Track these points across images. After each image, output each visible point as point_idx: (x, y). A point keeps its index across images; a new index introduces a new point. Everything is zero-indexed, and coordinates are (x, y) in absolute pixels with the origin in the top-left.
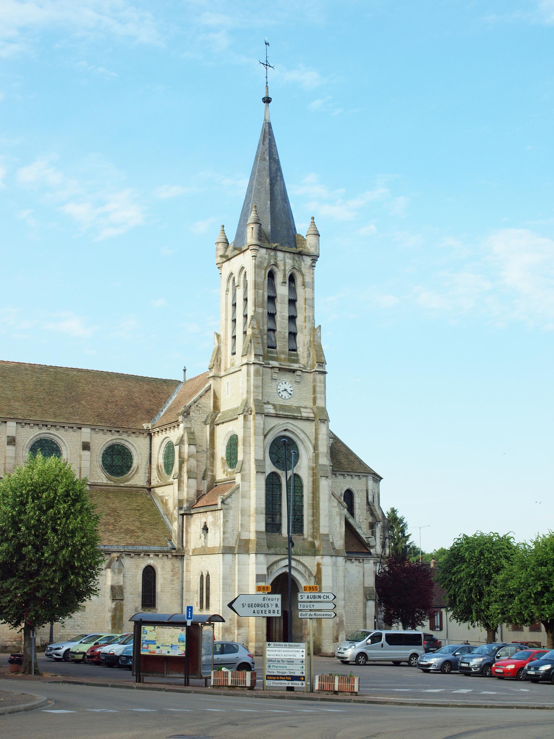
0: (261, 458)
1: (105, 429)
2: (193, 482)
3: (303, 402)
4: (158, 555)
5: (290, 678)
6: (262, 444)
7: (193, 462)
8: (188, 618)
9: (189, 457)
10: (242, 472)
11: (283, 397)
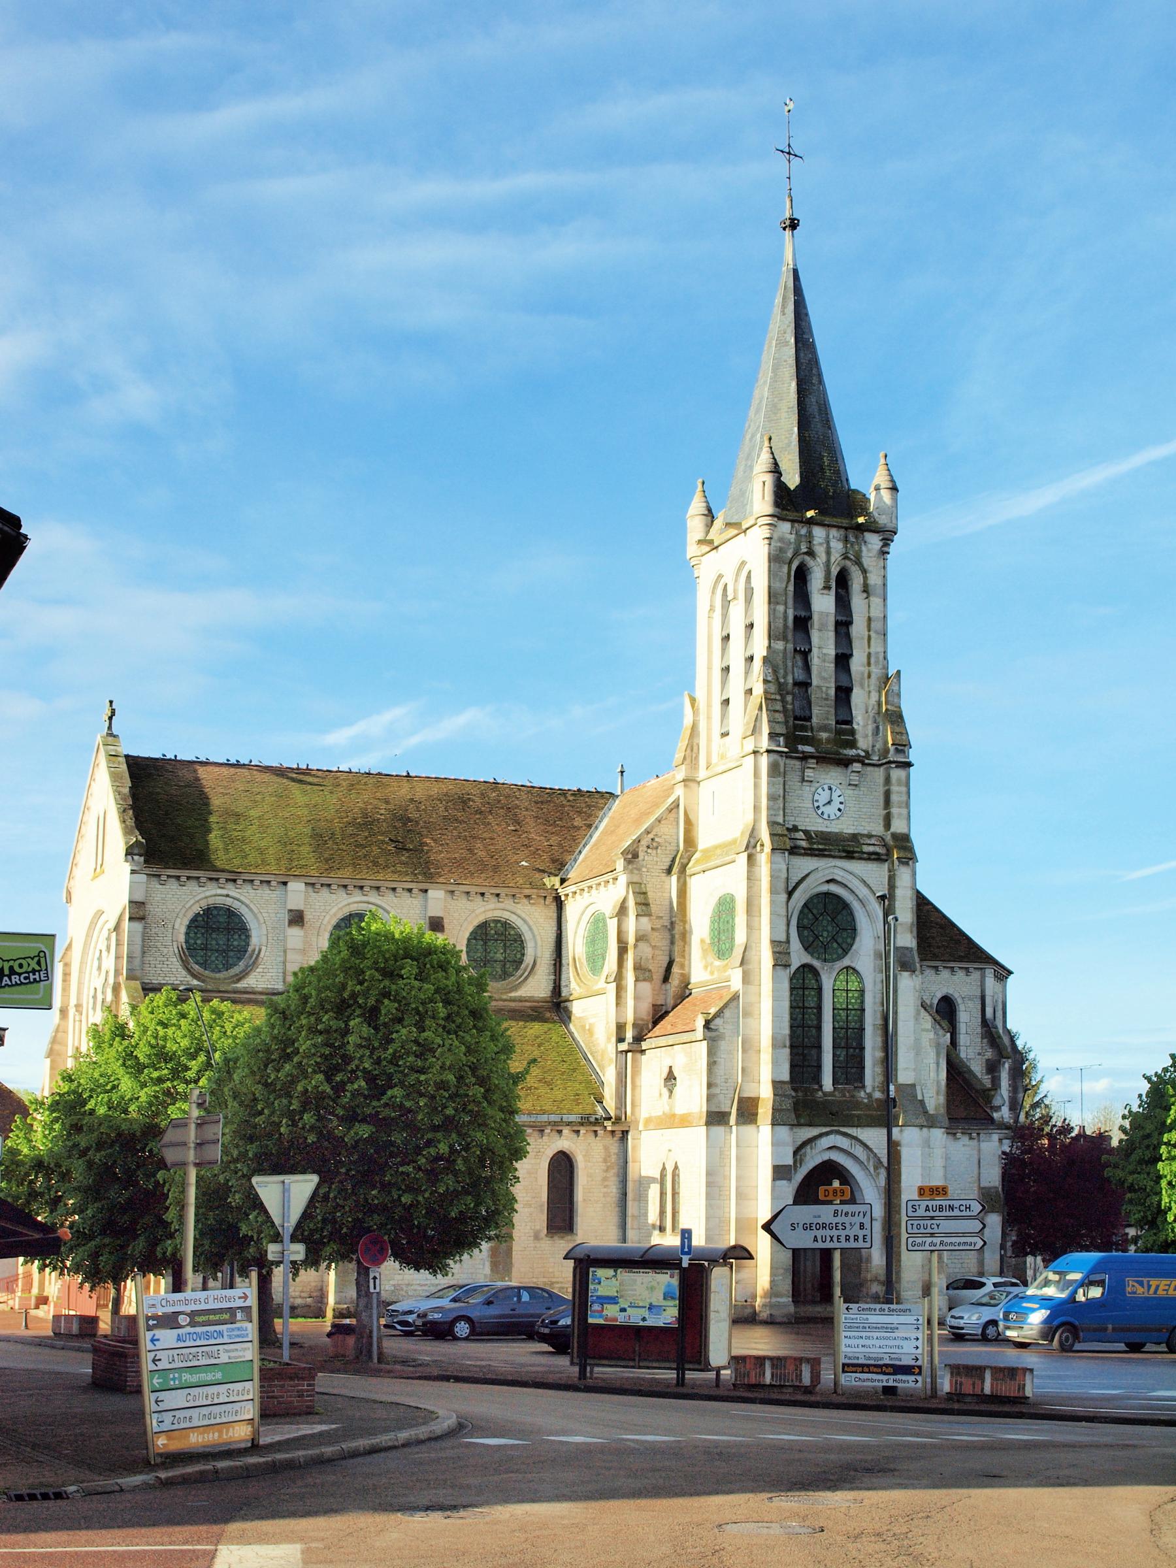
0: (783, 938)
1: (473, 889)
2: (646, 987)
5: (891, 1370)
6: (784, 910)
7: (646, 950)
8: (683, 1253)
9: (637, 940)
10: (745, 966)
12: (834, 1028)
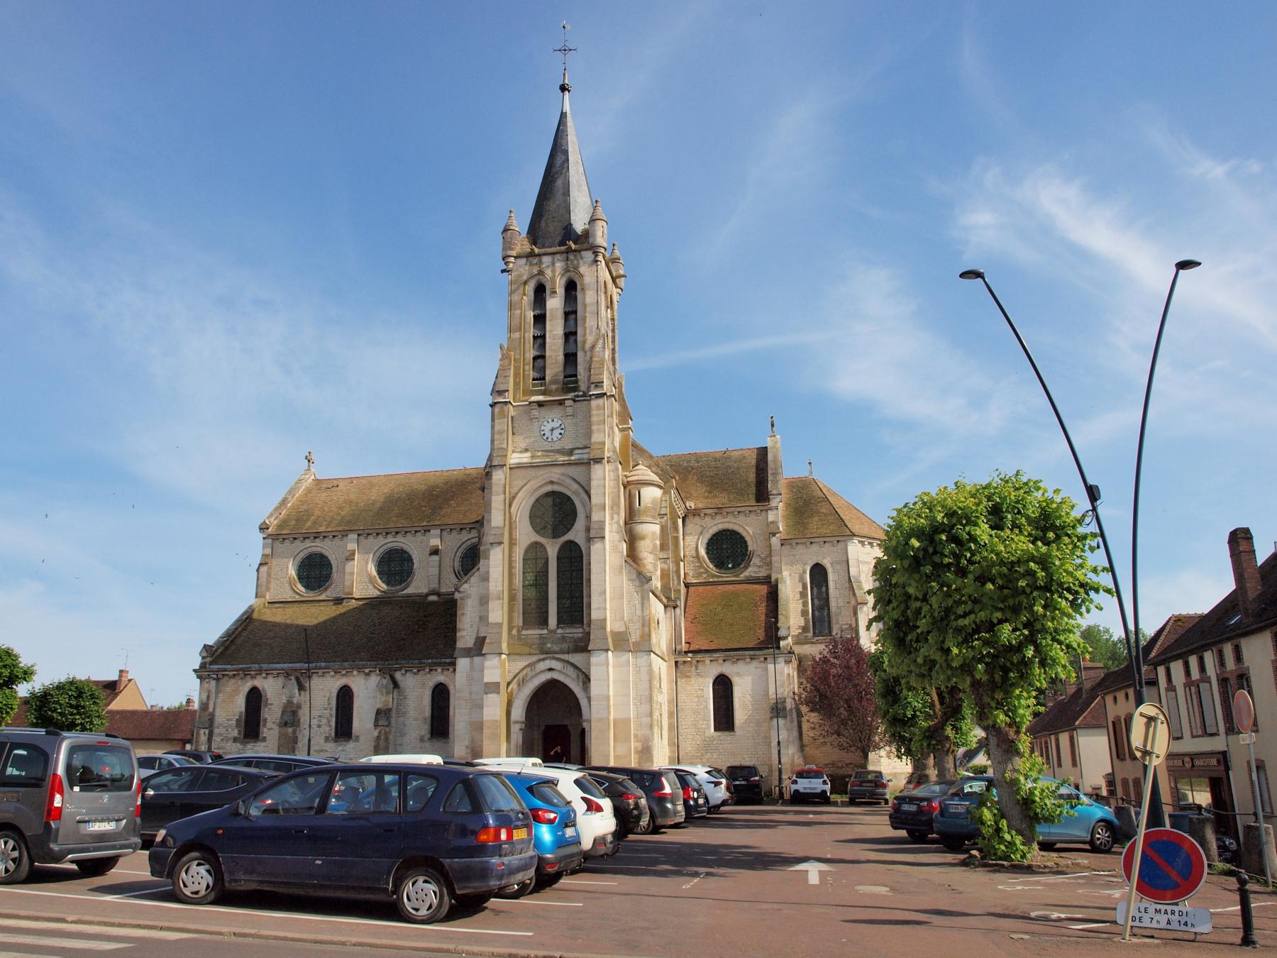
3: (581, 440)
4: (448, 670)
11: (550, 440)
12: (558, 586)
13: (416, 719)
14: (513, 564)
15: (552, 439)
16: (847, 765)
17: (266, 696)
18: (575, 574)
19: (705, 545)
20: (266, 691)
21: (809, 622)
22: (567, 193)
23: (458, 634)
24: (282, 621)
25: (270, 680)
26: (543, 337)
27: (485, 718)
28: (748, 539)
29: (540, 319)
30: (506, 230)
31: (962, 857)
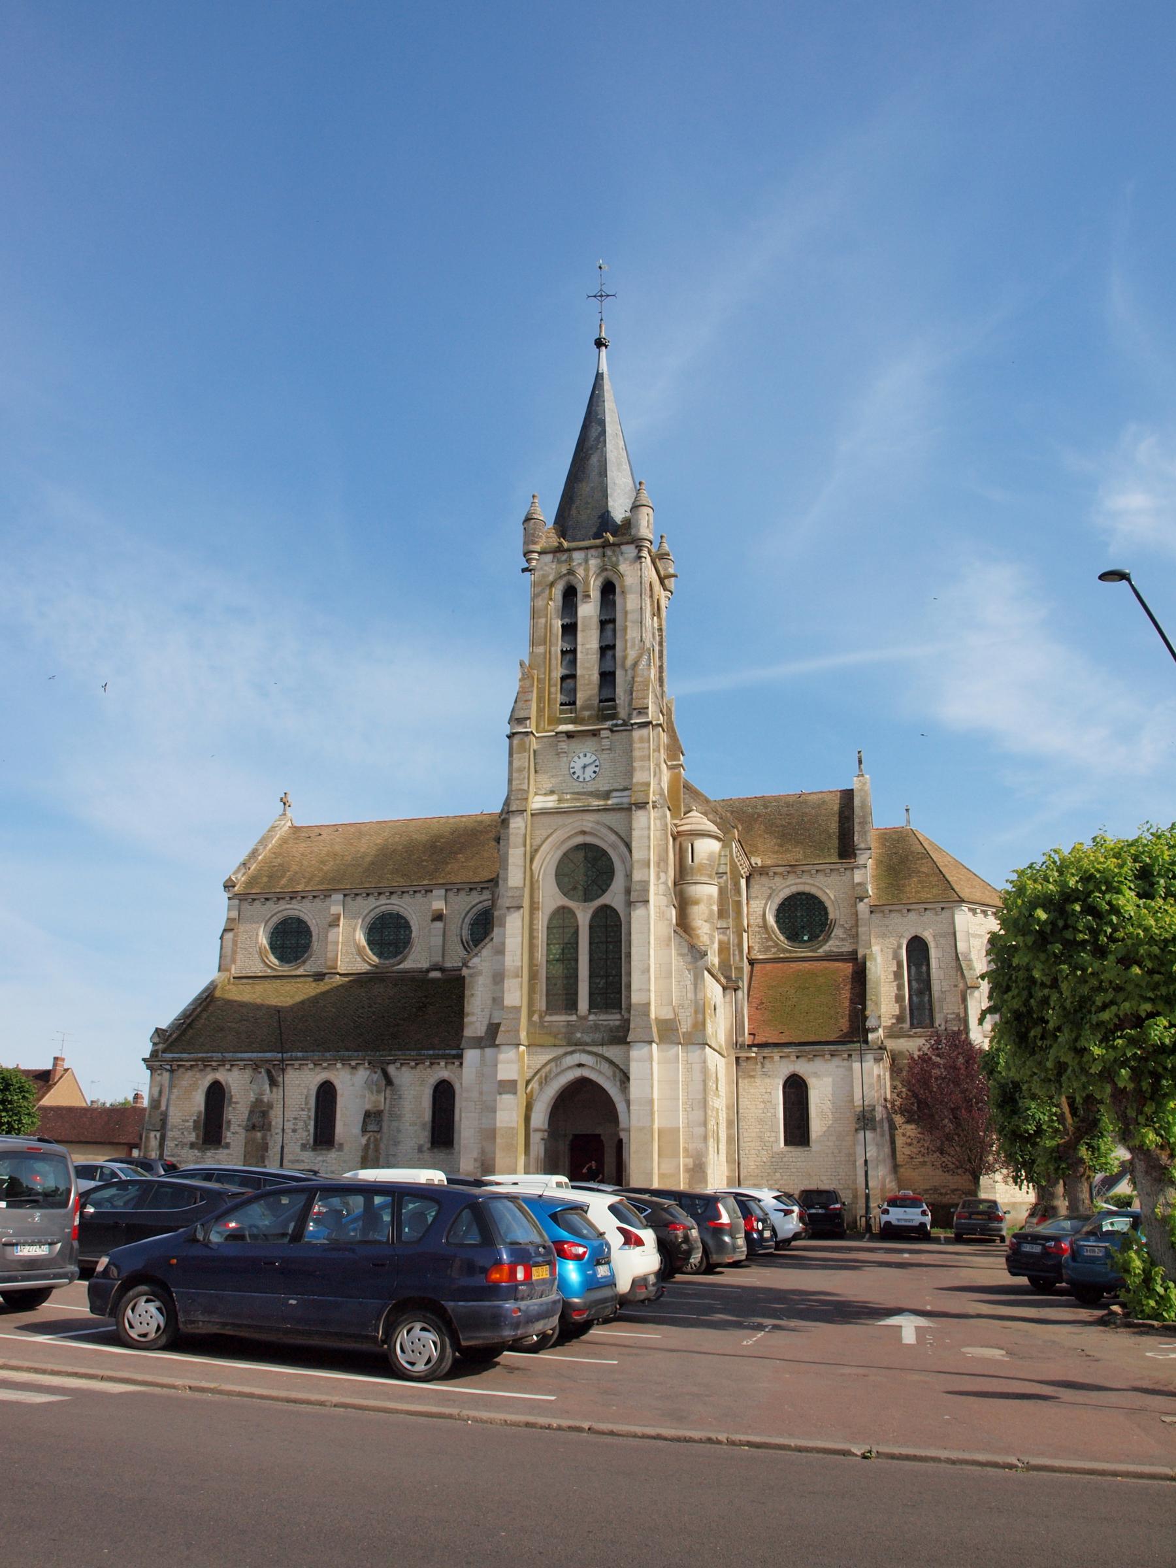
3: (619, 780)
4: (453, 1063)
12: (590, 960)
13: (413, 1124)
14: (535, 934)
15: (584, 779)
16: (954, 1191)
17: (230, 1093)
18: (611, 947)
19: (774, 912)
20: (230, 1087)
21: (905, 1009)
22: (603, 473)
23: (465, 1020)
24: (251, 1001)
25: (236, 1073)
26: (574, 652)
27: (498, 1125)
28: (828, 904)
29: (570, 630)
30: (528, 519)
31: (1100, 1313)
